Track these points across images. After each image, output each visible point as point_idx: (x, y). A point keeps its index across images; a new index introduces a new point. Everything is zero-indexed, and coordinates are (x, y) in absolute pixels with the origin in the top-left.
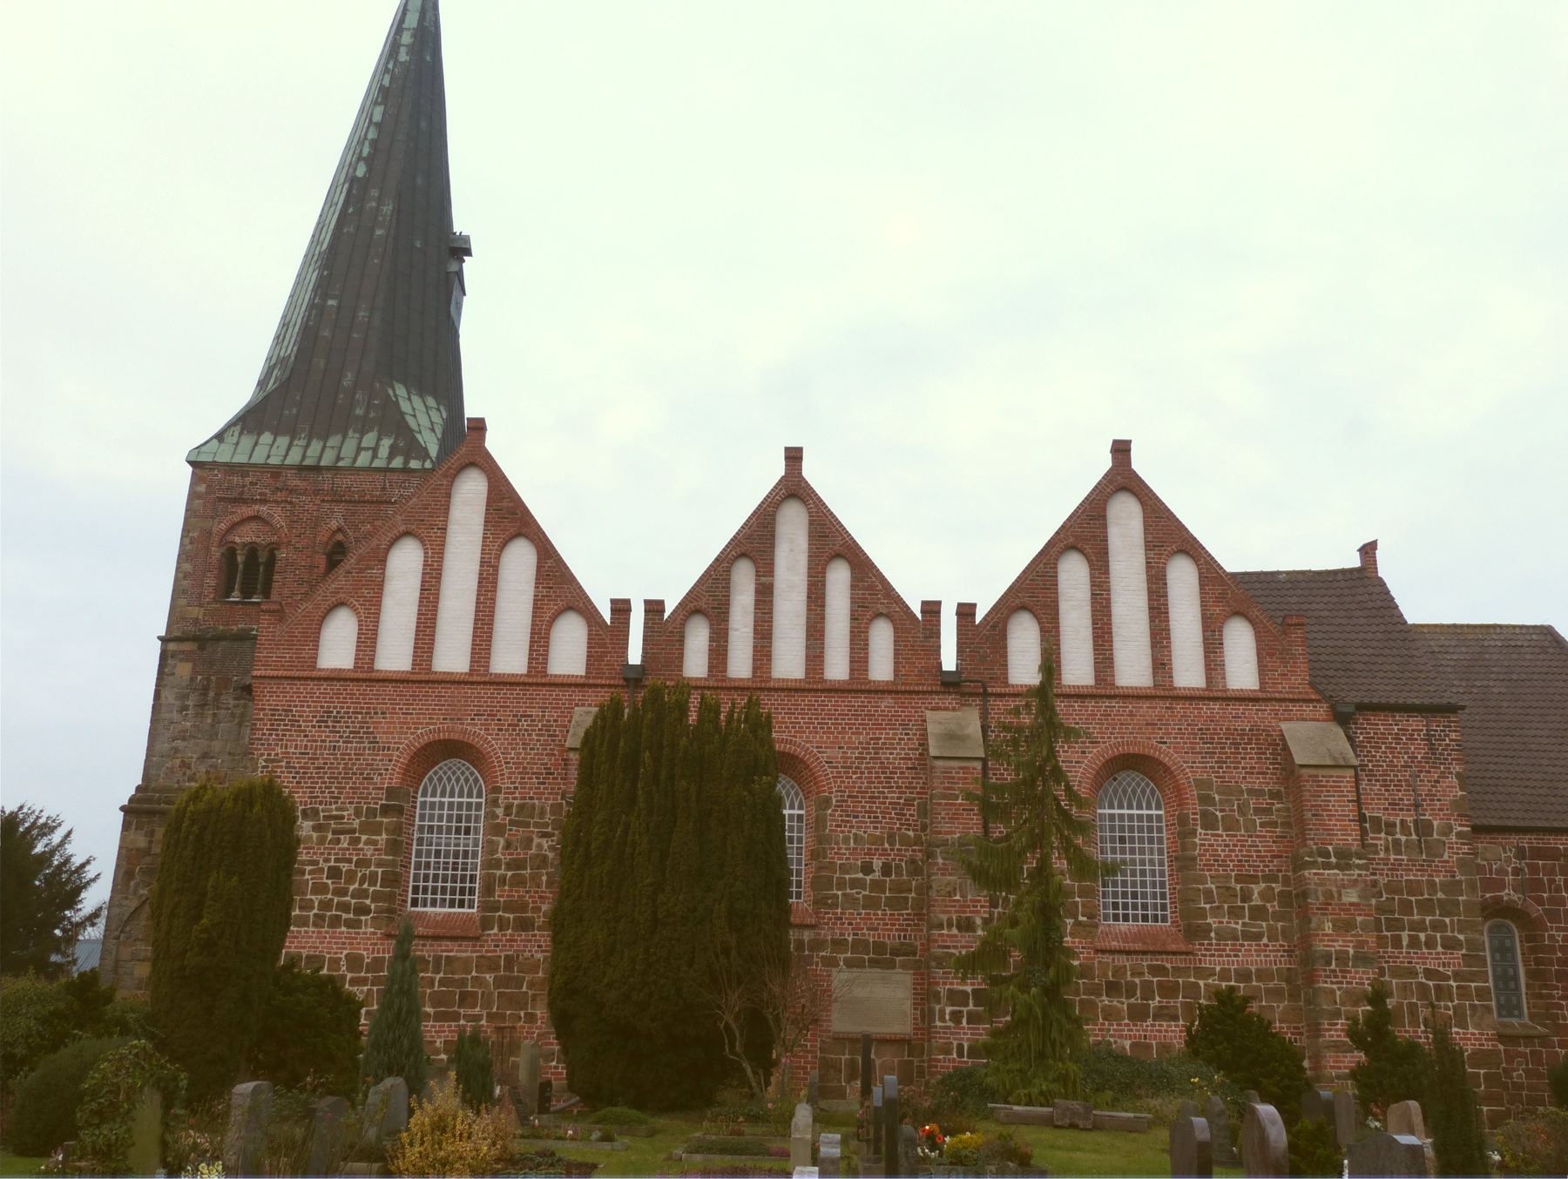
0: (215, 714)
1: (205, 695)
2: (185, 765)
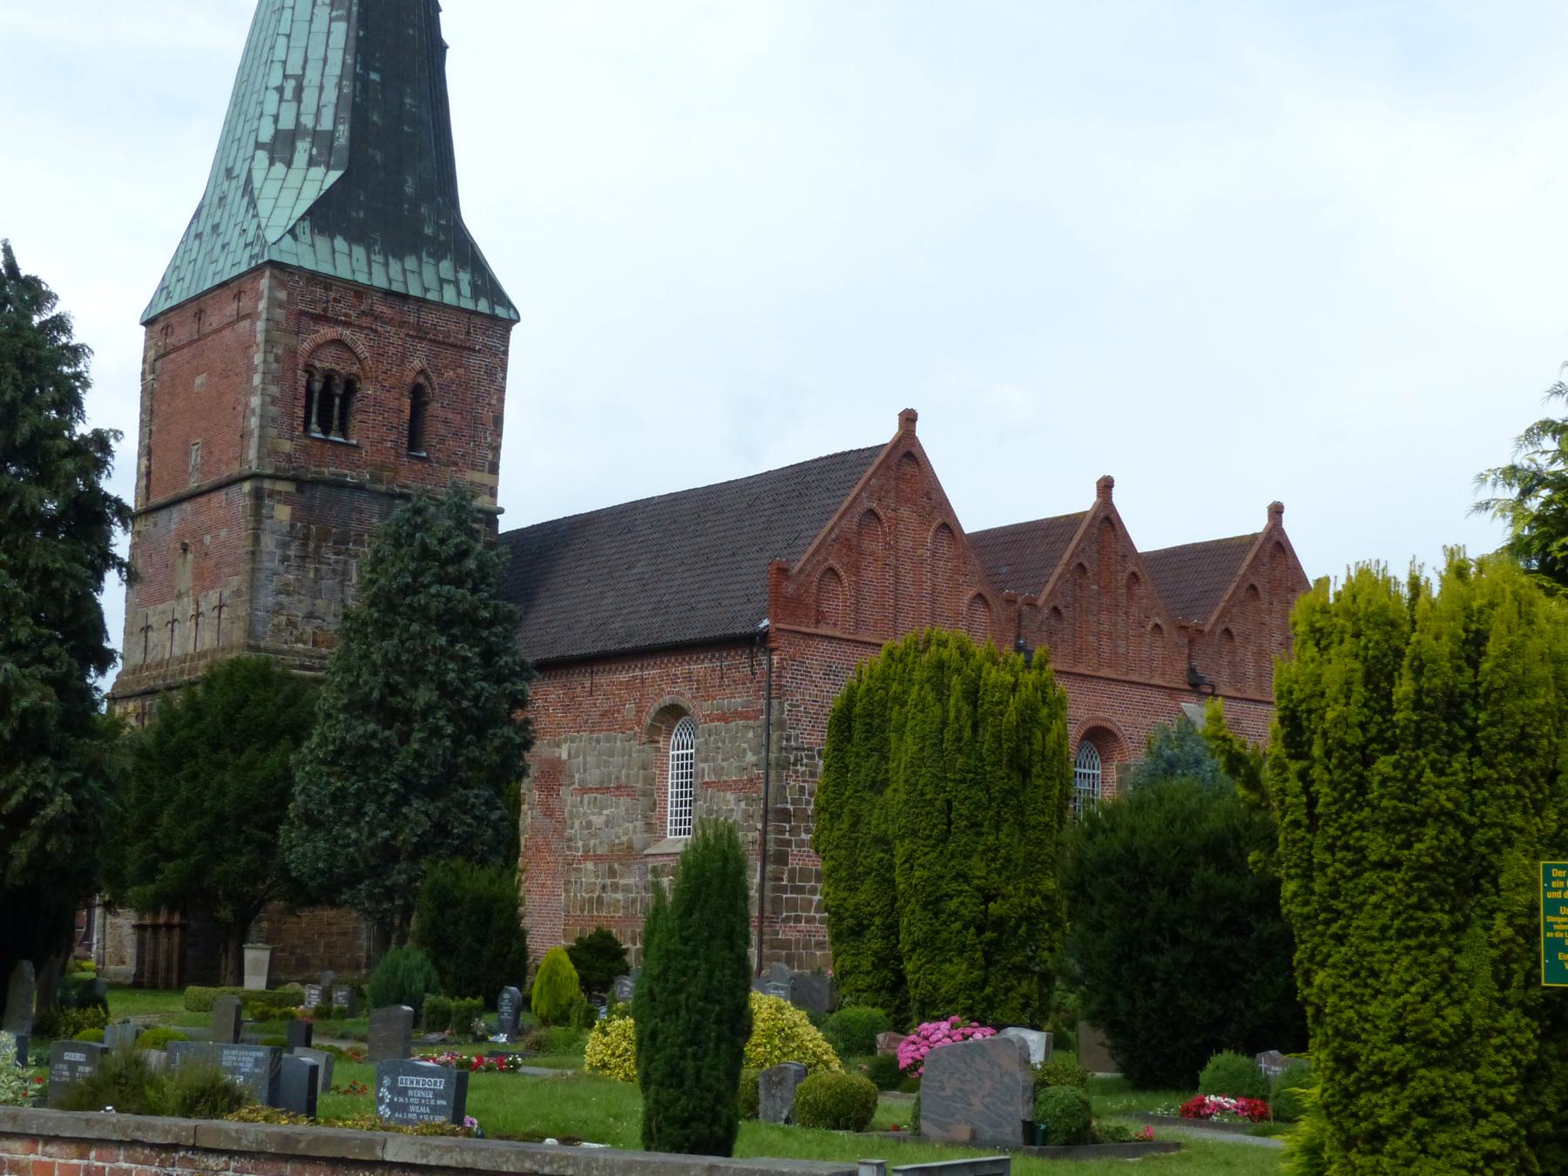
0: (317, 570)
1: (305, 545)
2: (291, 624)
